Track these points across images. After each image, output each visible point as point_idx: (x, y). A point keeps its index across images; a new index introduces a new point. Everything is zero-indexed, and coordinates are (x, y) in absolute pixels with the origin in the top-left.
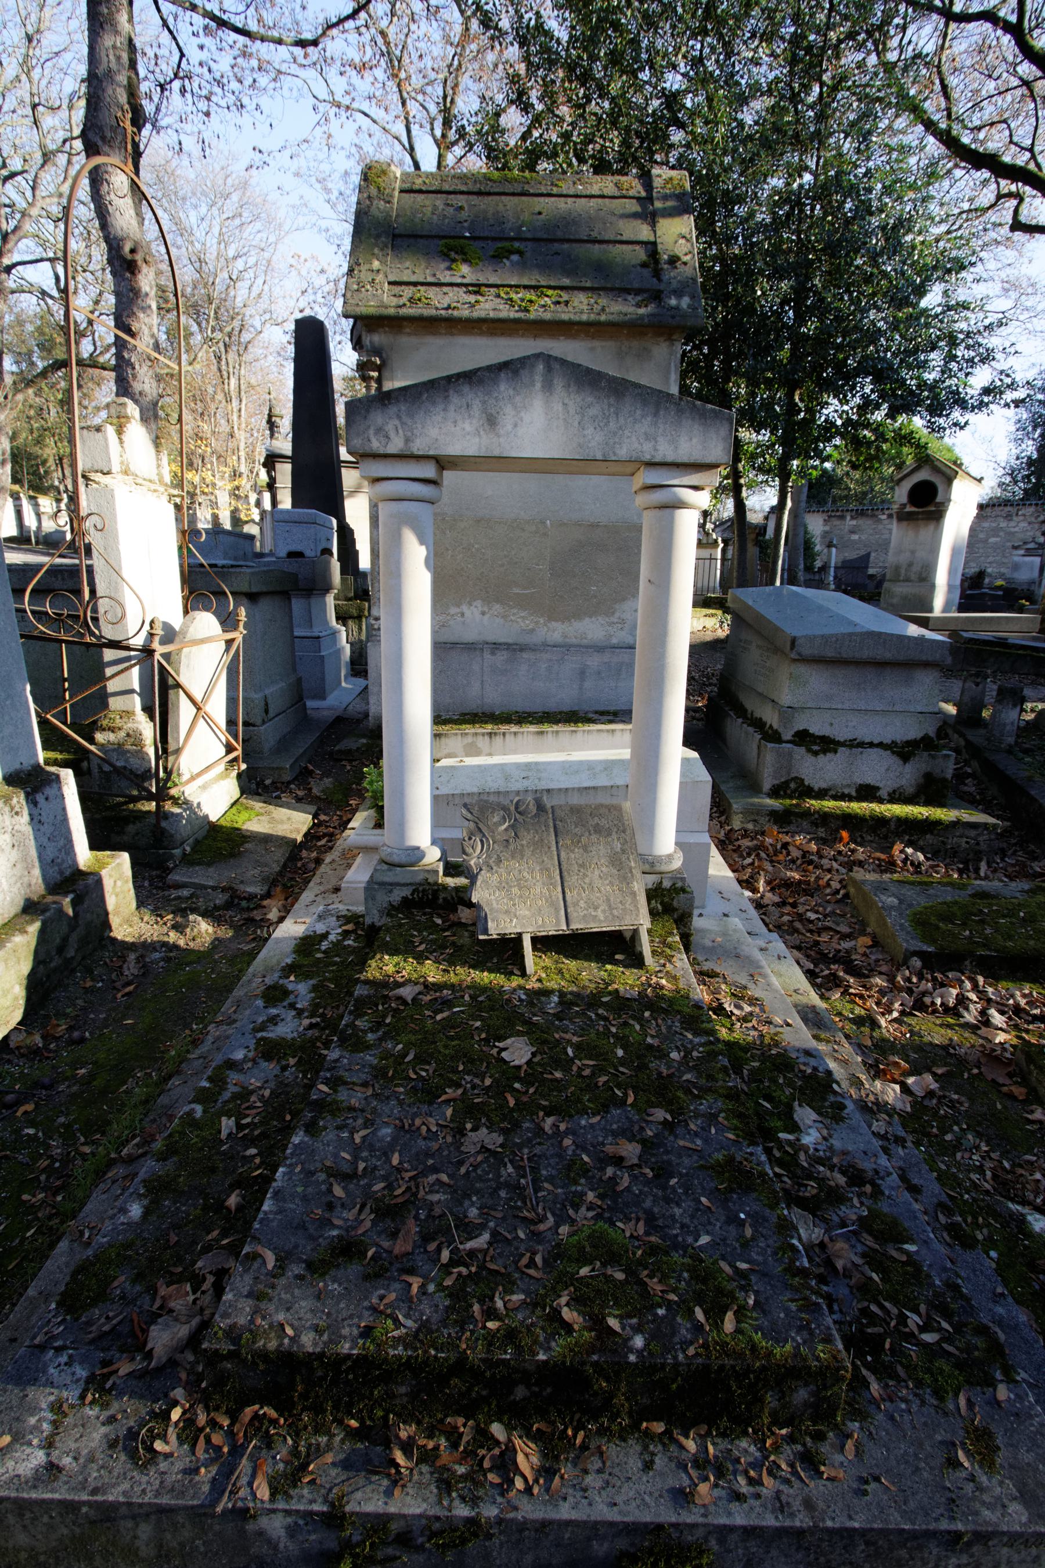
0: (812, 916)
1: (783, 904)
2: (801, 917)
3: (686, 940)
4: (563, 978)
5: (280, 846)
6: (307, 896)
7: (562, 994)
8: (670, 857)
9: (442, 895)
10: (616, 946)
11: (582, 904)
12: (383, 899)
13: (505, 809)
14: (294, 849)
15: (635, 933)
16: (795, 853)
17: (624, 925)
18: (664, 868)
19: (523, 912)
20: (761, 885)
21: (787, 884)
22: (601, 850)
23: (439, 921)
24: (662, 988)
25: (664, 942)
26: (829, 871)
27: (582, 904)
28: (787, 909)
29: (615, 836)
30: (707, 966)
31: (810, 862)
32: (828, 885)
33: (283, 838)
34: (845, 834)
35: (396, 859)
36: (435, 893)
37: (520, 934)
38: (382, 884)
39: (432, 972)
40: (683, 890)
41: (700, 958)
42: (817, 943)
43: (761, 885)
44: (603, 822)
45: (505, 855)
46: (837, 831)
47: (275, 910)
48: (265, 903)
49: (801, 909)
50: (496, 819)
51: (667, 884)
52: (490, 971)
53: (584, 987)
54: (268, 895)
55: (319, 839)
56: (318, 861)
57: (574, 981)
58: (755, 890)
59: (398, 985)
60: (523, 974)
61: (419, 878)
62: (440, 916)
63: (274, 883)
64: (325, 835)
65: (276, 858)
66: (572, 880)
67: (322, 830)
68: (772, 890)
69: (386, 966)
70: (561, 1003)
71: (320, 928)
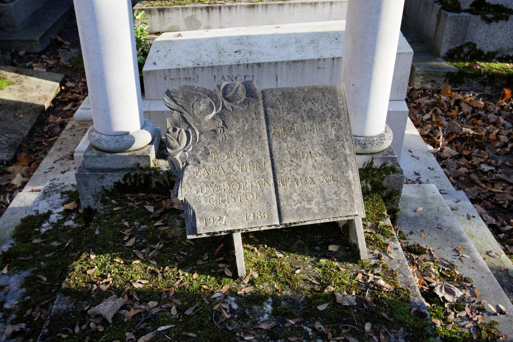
0: (486, 168)
1: (460, 156)
2: (475, 168)
3: (393, 214)
4: (277, 278)
5: (28, 113)
6: (47, 162)
7: (276, 302)
8: (381, 137)
9: (154, 180)
10: (329, 239)
11: (295, 197)
12: (96, 184)
13: (211, 95)
14: (41, 115)
15: (349, 225)
16: (466, 109)
17: (340, 217)
18: (376, 149)
19: (234, 208)
20: (441, 141)
21: (463, 138)
22: (314, 138)
23: (151, 209)
24: (380, 287)
25: (375, 227)
26: (495, 124)
27: (295, 197)
28: (463, 161)
29: (329, 122)
30: (413, 240)
31: (479, 117)
32: (498, 139)
33: (31, 105)
34: (507, 92)
35: (104, 145)
36: (148, 178)
37: (231, 233)
38: (93, 170)
39: (139, 276)
40: (393, 170)
41: (405, 232)
42: (493, 195)
43: (441, 141)
44: (317, 107)
45: (213, 147)
46: (501, 89)
47: (18, 175)
48: (10, 169)
49: (475, 161)
50: (202, 107)
51: (377, 164)
52: (201, 272)
53: (299, 291)
54: (14, 161)
55: (65, 104)
56: (62, 125)
57: (288, 281)
58: (435, 145)
59: (102, 296)
60: (235, 276)
61: (132, 162)
62: (152, 201)
63: (20, 149)
64: (70, 101)
65: (25, 124)
66: (284, 172)
67: (69, 96)
68: (450, 144)
69: (93, 268)
70: (275, 313)
71: (43, 207)
